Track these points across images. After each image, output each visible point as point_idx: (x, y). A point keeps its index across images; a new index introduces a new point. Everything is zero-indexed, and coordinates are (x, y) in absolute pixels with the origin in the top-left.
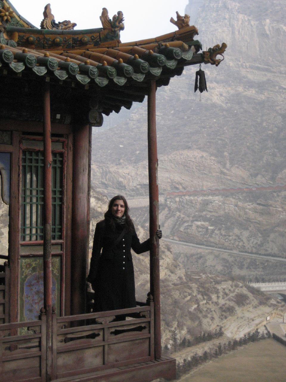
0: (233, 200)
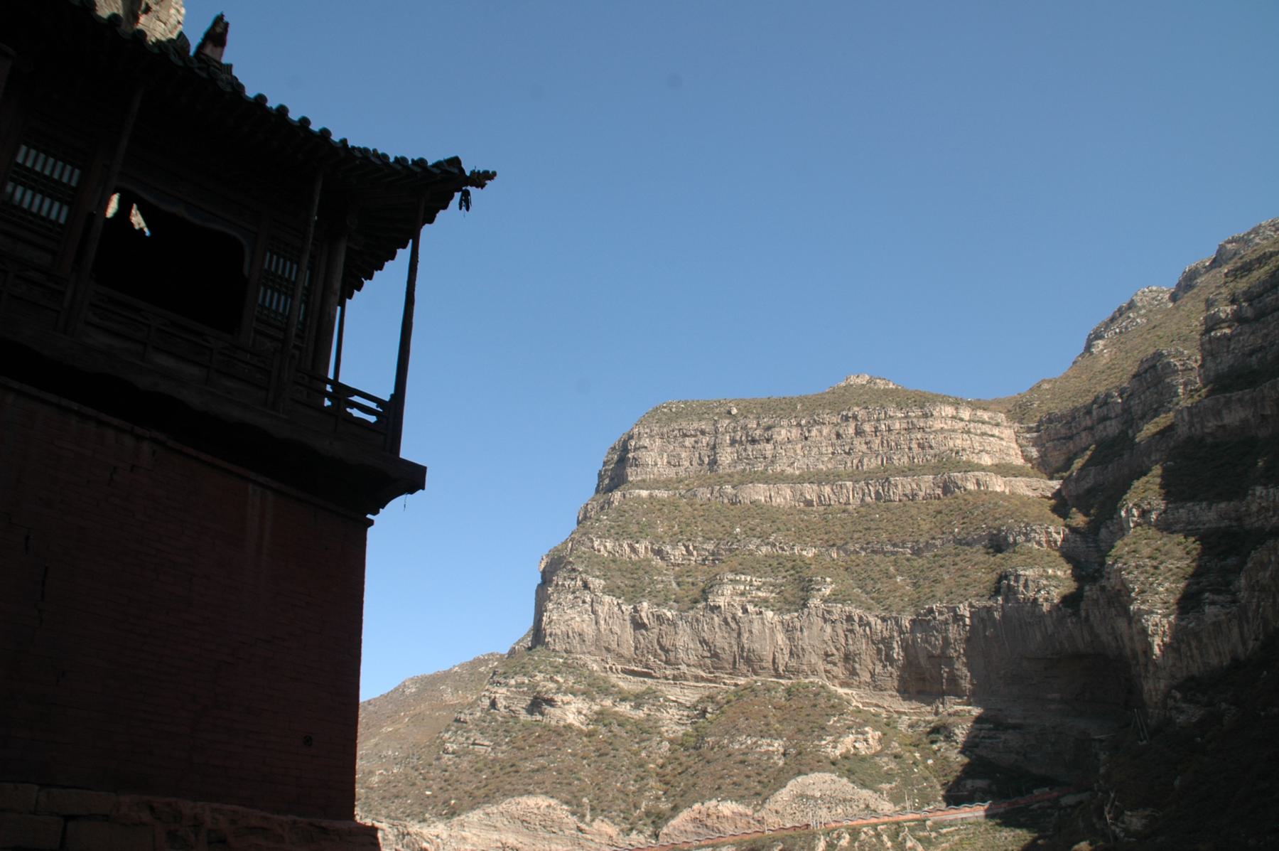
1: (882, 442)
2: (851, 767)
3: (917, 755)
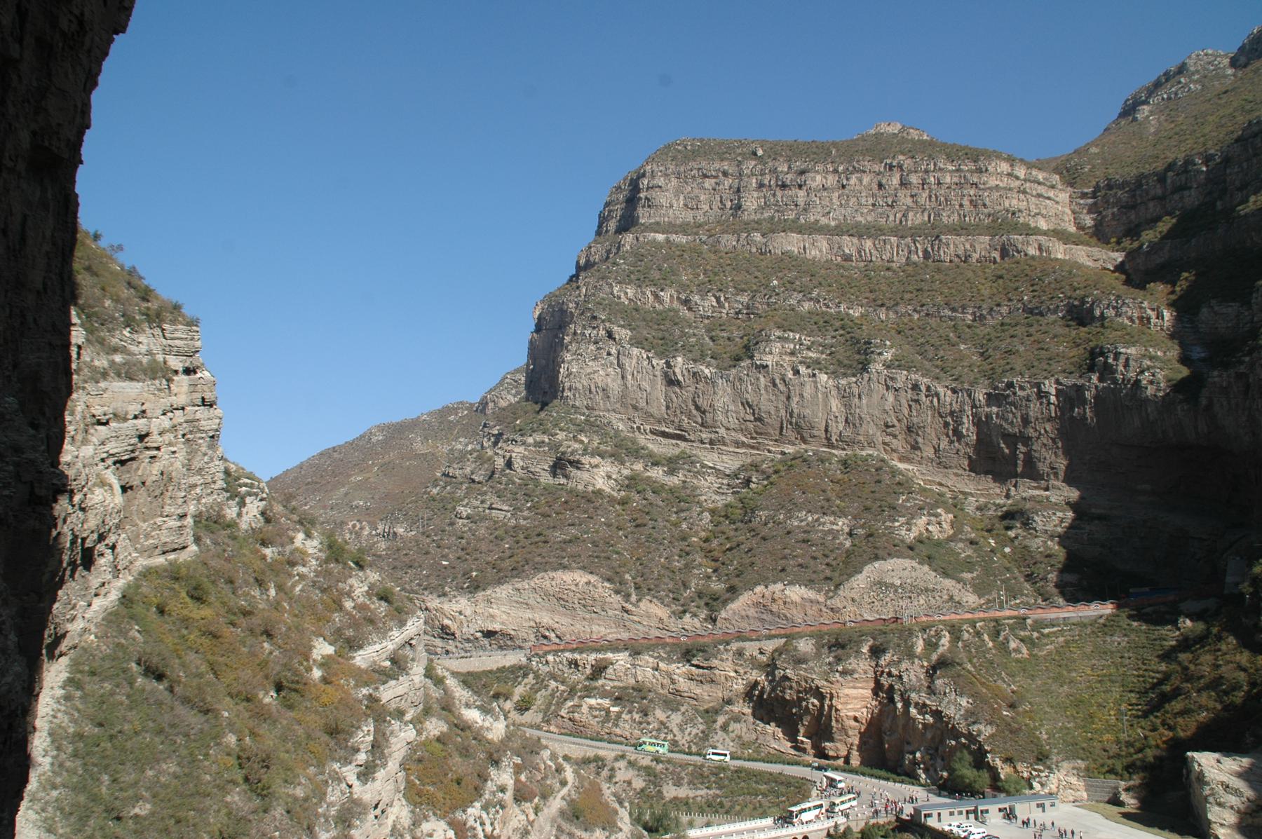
0: (651, 660)
1: (930, 197)
2: (924, 550)
3: (992, 541)
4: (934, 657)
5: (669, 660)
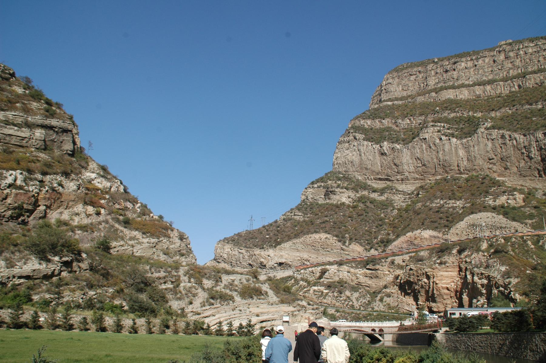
0: (347, 268)
4: (492, 251)
5: (357, 267)
